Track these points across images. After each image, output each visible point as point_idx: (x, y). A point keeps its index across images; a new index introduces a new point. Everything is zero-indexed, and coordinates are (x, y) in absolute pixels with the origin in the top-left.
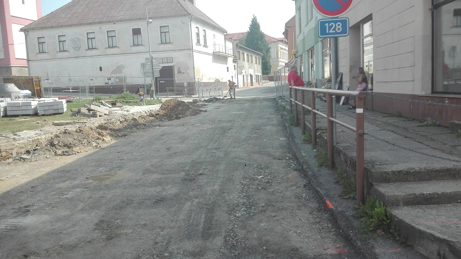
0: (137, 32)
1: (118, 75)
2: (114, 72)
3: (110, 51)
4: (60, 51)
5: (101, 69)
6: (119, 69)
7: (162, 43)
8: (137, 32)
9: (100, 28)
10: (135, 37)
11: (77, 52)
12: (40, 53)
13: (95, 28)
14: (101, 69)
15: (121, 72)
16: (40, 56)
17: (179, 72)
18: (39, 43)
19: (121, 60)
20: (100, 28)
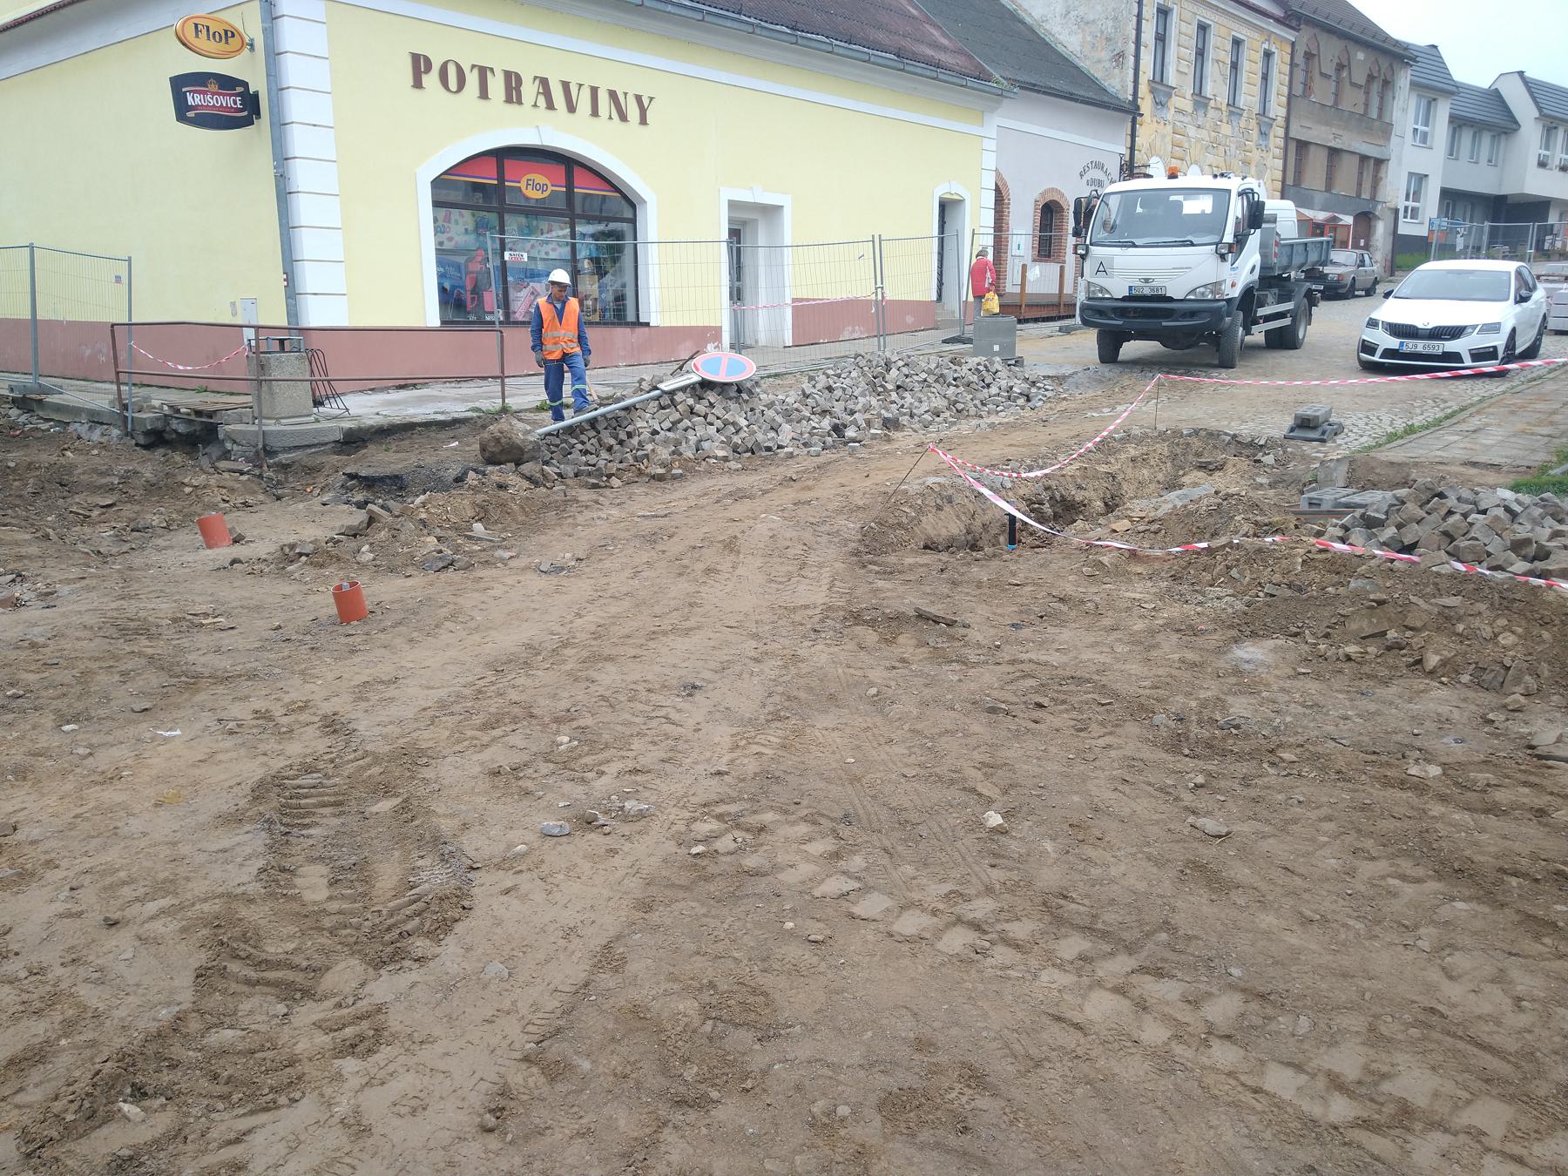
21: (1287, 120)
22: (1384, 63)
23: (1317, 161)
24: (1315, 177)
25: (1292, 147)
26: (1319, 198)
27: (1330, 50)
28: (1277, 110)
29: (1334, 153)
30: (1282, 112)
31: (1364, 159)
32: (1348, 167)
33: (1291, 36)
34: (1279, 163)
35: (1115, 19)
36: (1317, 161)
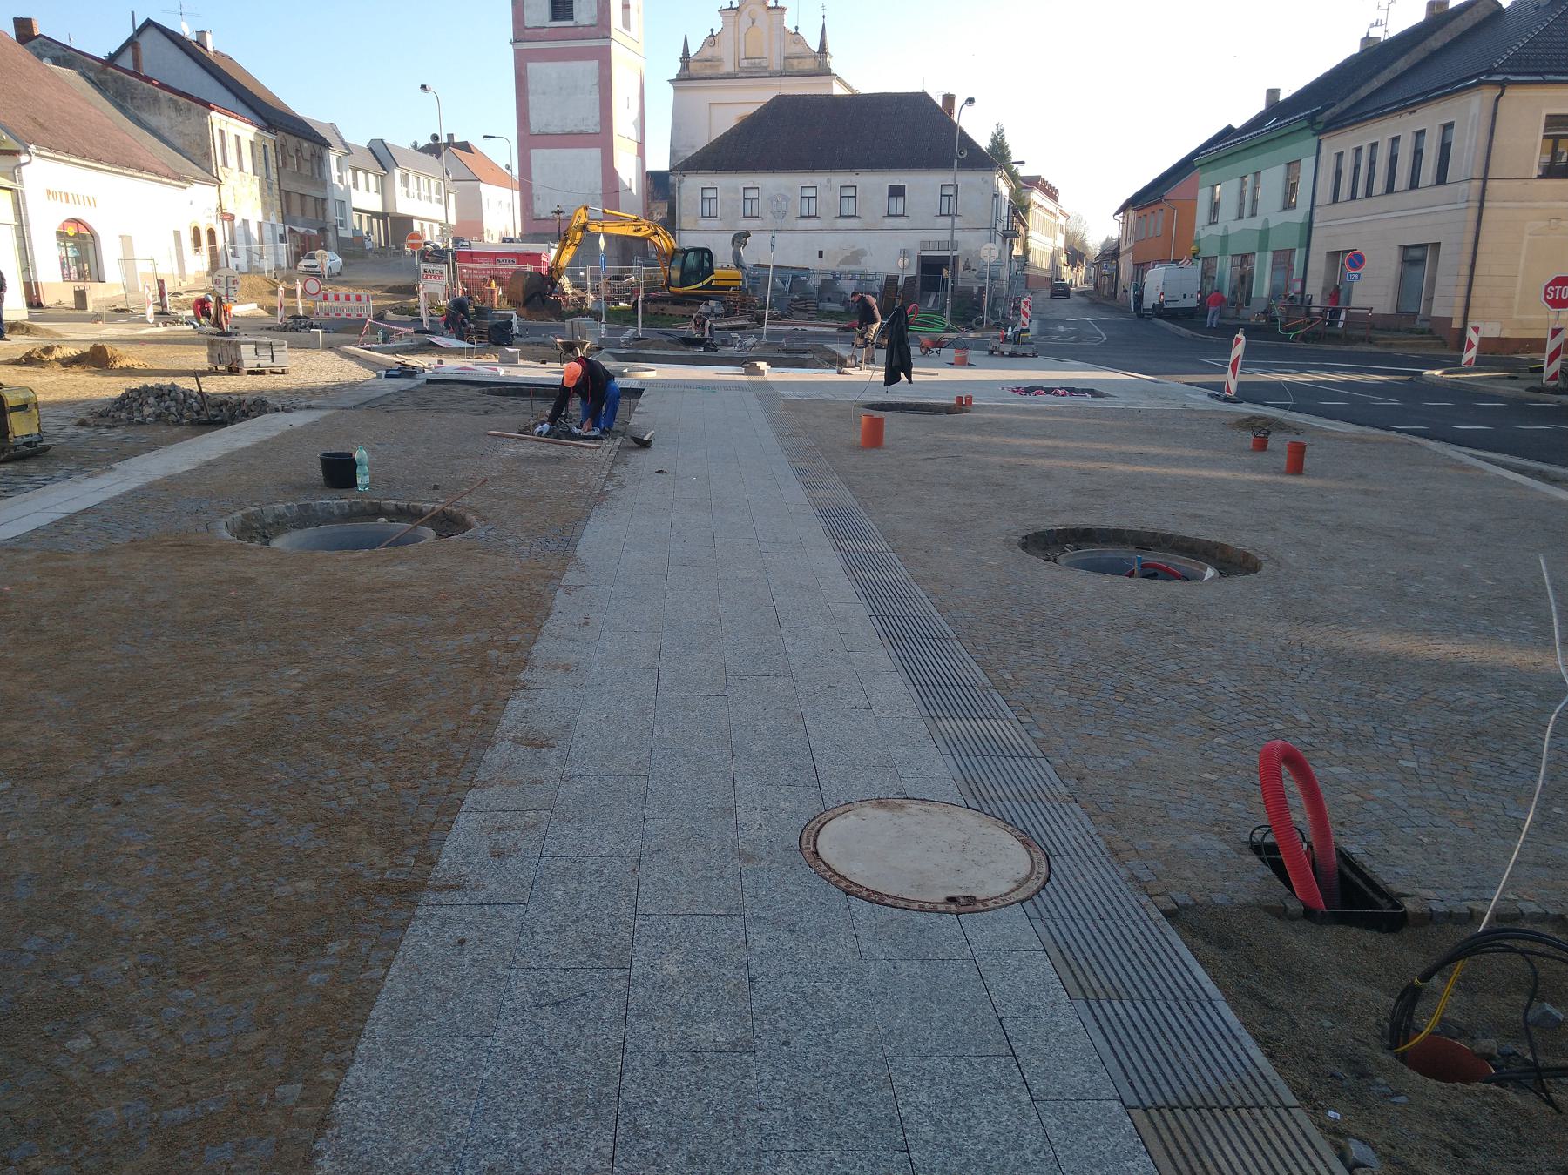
0: (897, 192)
1: (853, 268)
2: (846, 261)
3: (841, 223)
4: (744, 217)
5: (821, 254)
6: (857, 256)
7: (941, 215)
8: (897, 192)
9: (829, 181)
10: (893, 200)
11: (779, 221)
12: (703, 217)
13: (819, 179)
14: (821, 254)
15: (857, 262)
16: (703, 223)
17: (967, 267)
18: (703, 198)
19: (861, 240)
20: (829, 181)
21: (279, 180)
22: (317, 147)
23: (296, 201)
24: (296, 211)
25: (283, 193)
26: (300, 221)
27: (292, 141)
28: (274, 176)
29: (302, 196)
30: (275, 176)
31: (316, 199)
32: (310, 204)
33: (273, 137)
34: (279, 203)
35: (200, 136)
36: (296, 201)
